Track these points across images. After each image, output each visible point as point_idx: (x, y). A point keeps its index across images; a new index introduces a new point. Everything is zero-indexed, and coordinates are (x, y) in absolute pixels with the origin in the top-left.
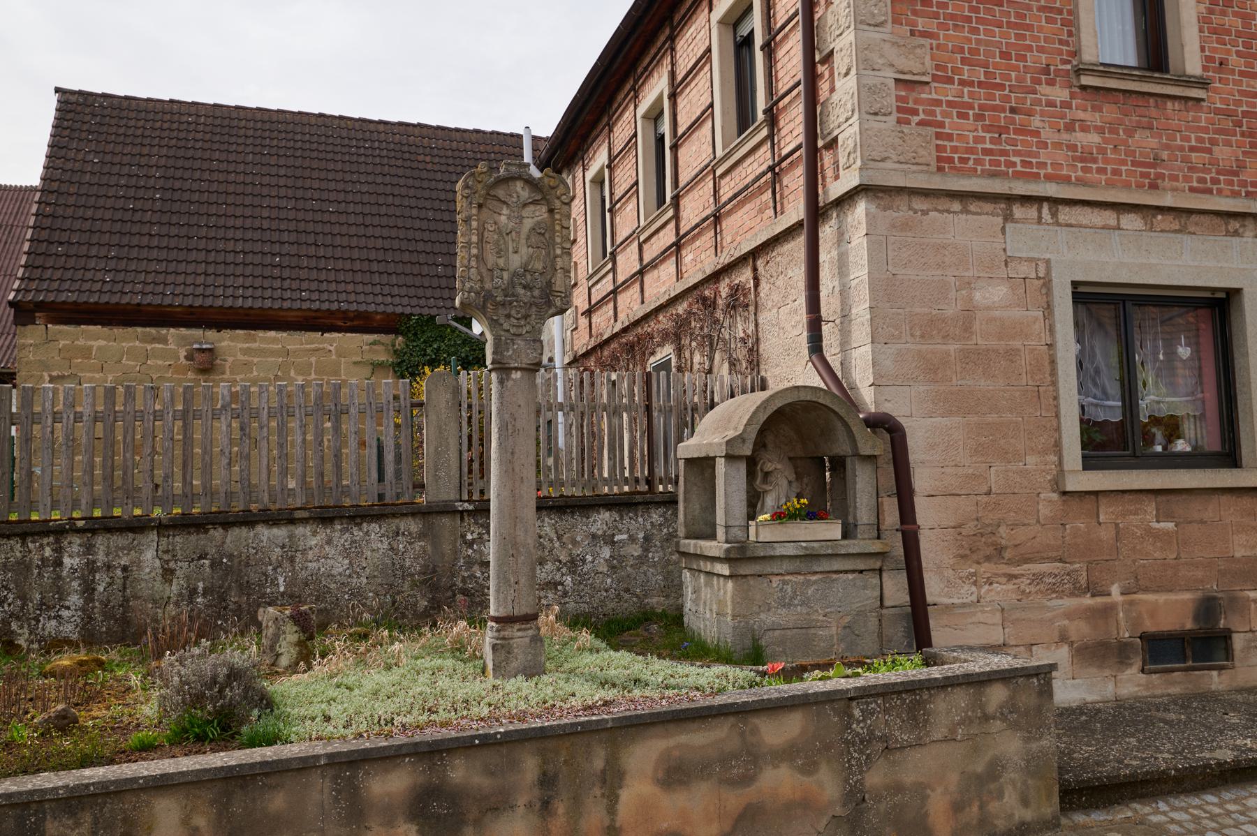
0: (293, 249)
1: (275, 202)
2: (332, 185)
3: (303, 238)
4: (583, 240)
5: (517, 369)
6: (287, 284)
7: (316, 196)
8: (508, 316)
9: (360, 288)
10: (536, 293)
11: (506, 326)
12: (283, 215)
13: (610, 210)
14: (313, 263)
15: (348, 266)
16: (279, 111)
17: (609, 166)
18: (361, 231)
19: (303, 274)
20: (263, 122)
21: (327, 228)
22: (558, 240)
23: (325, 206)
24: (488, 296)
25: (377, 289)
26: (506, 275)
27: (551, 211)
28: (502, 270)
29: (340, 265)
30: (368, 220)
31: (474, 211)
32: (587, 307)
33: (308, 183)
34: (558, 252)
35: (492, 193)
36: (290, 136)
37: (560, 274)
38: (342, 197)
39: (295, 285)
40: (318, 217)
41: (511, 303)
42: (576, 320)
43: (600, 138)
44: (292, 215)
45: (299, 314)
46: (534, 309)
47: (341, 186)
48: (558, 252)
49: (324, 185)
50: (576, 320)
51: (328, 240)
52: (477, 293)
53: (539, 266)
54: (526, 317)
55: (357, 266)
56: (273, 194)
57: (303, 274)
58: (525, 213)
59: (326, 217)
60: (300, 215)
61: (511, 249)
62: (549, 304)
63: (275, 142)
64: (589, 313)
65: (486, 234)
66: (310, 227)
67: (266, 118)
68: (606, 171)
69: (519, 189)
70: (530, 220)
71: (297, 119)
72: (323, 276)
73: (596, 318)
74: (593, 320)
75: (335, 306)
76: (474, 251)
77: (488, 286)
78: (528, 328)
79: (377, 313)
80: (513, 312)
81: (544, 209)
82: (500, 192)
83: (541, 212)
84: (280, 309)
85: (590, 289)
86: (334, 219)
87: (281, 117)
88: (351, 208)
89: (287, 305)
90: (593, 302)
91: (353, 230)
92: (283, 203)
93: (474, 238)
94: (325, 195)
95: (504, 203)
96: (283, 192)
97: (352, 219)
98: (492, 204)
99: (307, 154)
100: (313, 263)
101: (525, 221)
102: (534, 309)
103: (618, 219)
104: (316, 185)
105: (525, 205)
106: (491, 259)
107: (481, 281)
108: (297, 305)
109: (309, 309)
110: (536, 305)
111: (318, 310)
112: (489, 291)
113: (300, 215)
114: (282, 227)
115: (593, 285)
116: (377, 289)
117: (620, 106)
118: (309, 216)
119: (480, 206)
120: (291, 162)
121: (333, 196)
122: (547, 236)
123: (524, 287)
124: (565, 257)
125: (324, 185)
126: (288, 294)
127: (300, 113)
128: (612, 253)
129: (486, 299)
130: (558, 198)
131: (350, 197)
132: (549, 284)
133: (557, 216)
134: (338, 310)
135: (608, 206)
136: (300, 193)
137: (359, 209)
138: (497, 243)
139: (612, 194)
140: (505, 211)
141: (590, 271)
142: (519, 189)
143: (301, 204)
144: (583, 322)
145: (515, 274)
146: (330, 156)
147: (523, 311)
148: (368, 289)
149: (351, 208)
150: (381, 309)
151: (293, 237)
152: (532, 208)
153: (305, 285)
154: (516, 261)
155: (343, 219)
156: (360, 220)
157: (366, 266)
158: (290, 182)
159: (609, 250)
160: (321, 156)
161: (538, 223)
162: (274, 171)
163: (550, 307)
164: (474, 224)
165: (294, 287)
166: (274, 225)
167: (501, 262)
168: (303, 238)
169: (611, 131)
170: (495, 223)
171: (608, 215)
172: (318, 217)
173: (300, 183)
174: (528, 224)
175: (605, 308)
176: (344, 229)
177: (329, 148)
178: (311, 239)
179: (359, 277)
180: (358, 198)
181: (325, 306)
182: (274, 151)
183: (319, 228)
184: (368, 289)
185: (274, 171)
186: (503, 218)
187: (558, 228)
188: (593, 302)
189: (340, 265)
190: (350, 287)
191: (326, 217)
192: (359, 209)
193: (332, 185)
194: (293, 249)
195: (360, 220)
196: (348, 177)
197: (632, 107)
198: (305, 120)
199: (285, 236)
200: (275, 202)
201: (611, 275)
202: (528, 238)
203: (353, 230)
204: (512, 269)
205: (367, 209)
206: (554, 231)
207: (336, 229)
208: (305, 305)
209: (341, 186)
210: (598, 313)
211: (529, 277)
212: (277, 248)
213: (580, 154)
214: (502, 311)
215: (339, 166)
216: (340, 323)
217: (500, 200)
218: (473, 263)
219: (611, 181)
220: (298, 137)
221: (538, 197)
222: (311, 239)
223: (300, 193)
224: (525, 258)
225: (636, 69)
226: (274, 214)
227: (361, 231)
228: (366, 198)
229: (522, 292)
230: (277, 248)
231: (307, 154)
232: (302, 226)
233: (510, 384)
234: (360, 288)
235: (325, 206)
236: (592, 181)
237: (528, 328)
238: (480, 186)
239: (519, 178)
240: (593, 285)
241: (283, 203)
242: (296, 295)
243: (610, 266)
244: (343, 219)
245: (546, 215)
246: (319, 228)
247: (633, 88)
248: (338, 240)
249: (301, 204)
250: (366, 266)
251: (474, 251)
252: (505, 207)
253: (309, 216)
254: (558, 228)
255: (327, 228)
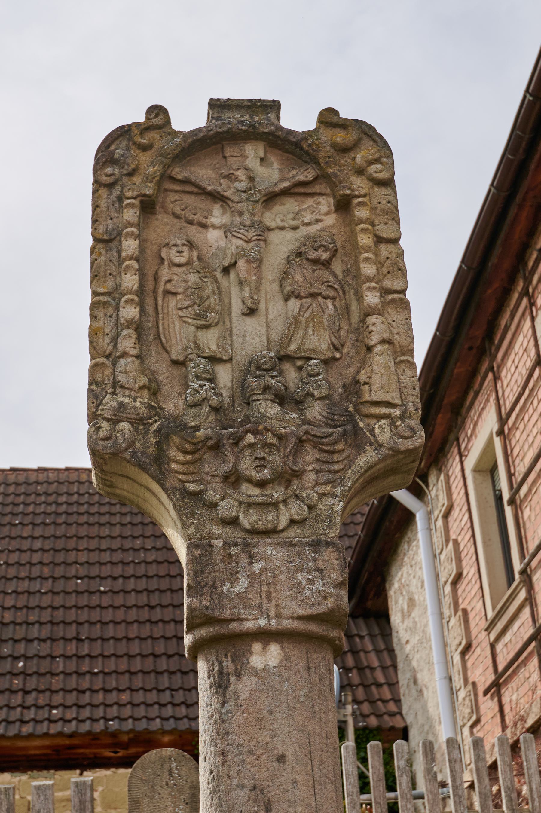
0: (45, 649)
1: (24, 585)
2: (106, 557)
3: (60, 631)
4: (474, 570)
5: (265, 636)
6: (30, 699)
7: (82, 572)
8: (233, 479)
9: (139, 697)
10: (316, 411)
11: (227, 508)
12: (34, 601)
13: (512, 501)
14: (72, 666)
15: (123, 666)
16: (41, 470)
17: (500, 432)
18: (145, 614)
19: (57, 683)
20: (17, 484)
21: (95, 615)
22: (368, 269)
23: (93, 585)
24: (176, 427)
25: (166, 697)
26: (225, 375)
27: (343, 206)
28: (214, 360)
29: (111, 664)
30: (155, 600)
31: (131, 215)
32: (491, 677)
33: (72, 557)
34: (372, 298)
35: (179, 172)
36: (52, 499)
37: (381, 358)
38: (118, 570)
39: (42, 700)
40: (84, 600)
41: (237, 440)
42: (476, 707)
43: (481, 398)
44: (46, 601)
45: (47, 742)
46: (310, 455)
47: (118, 556)
48: (372, 298)
49: (94, 557)
50: (476, 707)
51: (97, 631)
52: (139, 422)
53: (319, 341)
54: (288, 477)
55: (137, 664)
56: (23, 574)
57: (57, 683)
58: (272, 217)
59: (95, 600)
60: (58, 601)
61: (237, 307)
62: (357, 439)
63: (31, 508)
64: (496, 688)
65: (165, 273)
66: (72, 615)
67: (21, 478)
68: (497, 441)
69: (253, 162)
70: (289, 235)
71: (63, 477)
72: (85, 684)
73: (510, 695)
74: (506, 699)
75: (99, 727)
76: (130, 312)
77: (173, 405)
78: (295, 509)
79: (164, 732)
80: (247, 465)
81: (325, 204)
82: (204, 173)
83: (318, 214)
84: (17, 736)
85: (493, 646)
86: (106, 601)
87: (42, 477)
88: (131, 584)
89: (27, 729)
90: (500, 668)
91: (133, 615)
92: (36, 586)
93: (130, 281)
94: (95, 571)
95: (217, 197)
96: (36, 571)
97: (132, 599)
98: (175, 201)
99: (73, 519)
100: (72, 666)
101: (274, 237)
102: (310, 455)
103: (527, 513)
104: (83, 557)
105: (271, 198)
106: (179, 333)
107: (154, 389)
108: (43, 728)
109: (60, 734)
110: (317, 442)
111: (72, 736)
112: (175, 418)
113: (58, 601)
114: (32, 619)
115: (498, 638)
116: (166, 697)
117: (507, 328)
118: (72, 600)
119: (148, 206)
120: (50, 531)
121: (106, 571)
122: (338, 267)
123: (281, 399)
124: (393, 314)
125: (94, 557)
126: (31, 714)
127: (67, 469)
128: (523, 572)
129: (163, 436)
130: (360, 172)
131: (130, 570)
132: (354, 387)
133: (361, 213)
134: (105, 732)
135: (506, 496)
136: (59, 571)
137: (142, 584)
138: (197, 296)
139: (510, 476)
140: (218, 216)
141: (490, 614)
142: (253, 162)
143: (60, 586)
144: (488, 706)
145: (256, 366)
146: (104, 519)
147: (276, 460)
148: (152, 697)
149: (131, 584)
150: (170, 725)
151: (45, 632)
152: (290, 205)
153: (58, 699)
154: (252, 338)
155: (119, 600)
156: (143, 599)
157: (149, 664)
158: (47, 558)
159: (517, 566)
160: (92, 520)
161: (313, 242)
162: (26, 545)
163: (359, 447)
164: (130, 246)
165: (41, 702)
166: (20, 616)
167: (210, 340)
168: (60, 631)
169: (496, 378)
170: (191, 245)
171: (508, 511)
172: (84, 600)
173: (60, 557)
174: (282, 244)
175: (523, 673)
176: (120, 615)
177: (103, 509)
178: (71, 631)
179: (138, 681)
180: (141, 570)
181: (86, 727)
182: (28, 520)
183: (84, 616)
184: (152, 697)
185: (26, 545)
186: (214, 236)
187: (365, 240)
188: (500, 668)
189: (111, 664)
190: (125, 697)
191: (95, 600)
192: (142, 584)
193: (106, 557)
194: (45, 649)
195: (143, 599)
196: (128, 544)
197: (528, 323)
198: (73, 477)
199: (35, 632)
200: (24, 585)
201: (527, 611)
202: (286, 274)
203: (133, 615)
204: (241, 355)
205: (154, 584)
206: (354, 250)
207: (108, 615)
208: (55, 729)
209: (118, 556)
210: (513, 684)
211: (291, 375)
212: (21, 648)
213: (452, 437)
214: (213, 467)
215: (117, 531)
216: (108, 753)
217: (203, 192)
218: (128, 343)
219: (507, 461)
220: (64, 499)
221: (308, 174)
222: (71, 631)
223: (59, 571)
224: (279, 328)
225: (526, 264)
226: (22, 601)
227: (145, 614)
228: (153, 570)
229: (275, 409)
230: (21, 648)
231: (73, 519)
232: (59, 615)
233: (245, 687)
234: (139, 697)
235: (93, 585)
236: (476, 470)
237: (295, 509)
238: (144, 158)
239: (251, 134)
240: (498, 638)
241: (36, 586)
242: (43, 714)
243: (523, 594)
244: (119, 600)
245: (331, 220)
246: (84, 616)
247: (525, 293)
248: (110, 631)
249: (60, 586)
250: (149, 664)
251: (130, 312)
252: (217, 210)
253: (72, 600)
254: (365, 240)
255: (95, 615)
